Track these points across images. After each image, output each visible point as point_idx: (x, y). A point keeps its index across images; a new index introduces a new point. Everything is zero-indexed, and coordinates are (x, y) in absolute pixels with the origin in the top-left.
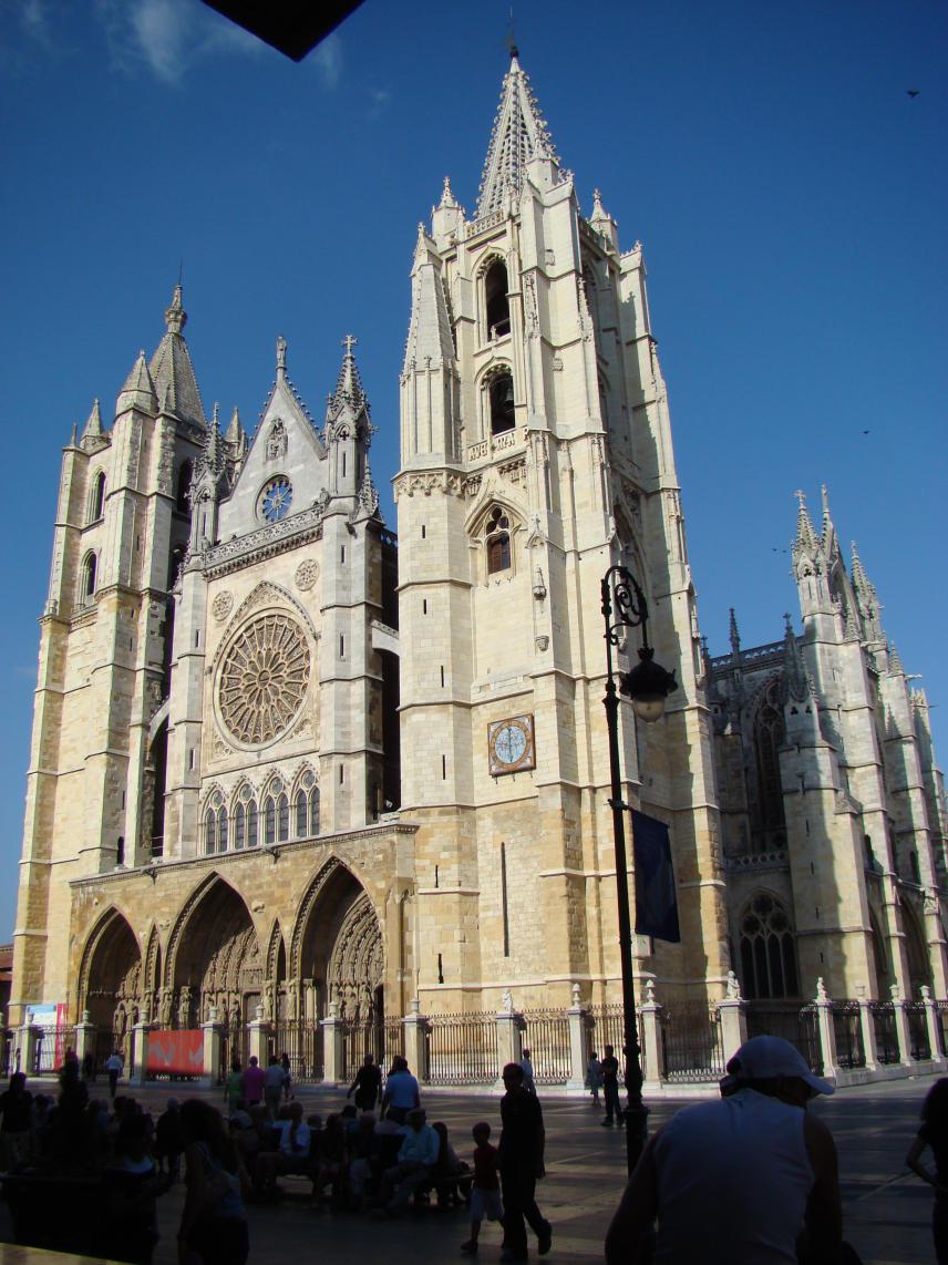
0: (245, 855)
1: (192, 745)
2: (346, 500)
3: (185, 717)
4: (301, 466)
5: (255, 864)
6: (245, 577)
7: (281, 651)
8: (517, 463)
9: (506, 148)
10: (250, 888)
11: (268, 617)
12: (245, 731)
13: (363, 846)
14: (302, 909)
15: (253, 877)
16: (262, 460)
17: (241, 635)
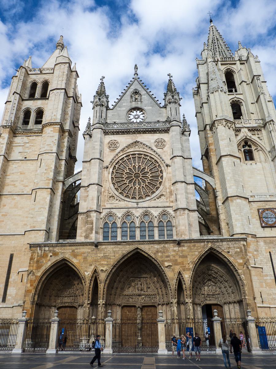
0: (159, 242)
1: (99, 194)
2: (179, 123)
3: (96, 182)
4: (151, 108)
5: (164, 246)
6: (125, 137)
7: (146, 167)
8: (255, 129)
9: (212, 45)
10: (162, 257)
11: (138, 154)
12: (127, 194)
13: (229, 245)
14: (194, 268)
15: (164, 252)
16: (129, 101)
17: (124, 158)
